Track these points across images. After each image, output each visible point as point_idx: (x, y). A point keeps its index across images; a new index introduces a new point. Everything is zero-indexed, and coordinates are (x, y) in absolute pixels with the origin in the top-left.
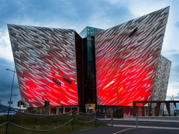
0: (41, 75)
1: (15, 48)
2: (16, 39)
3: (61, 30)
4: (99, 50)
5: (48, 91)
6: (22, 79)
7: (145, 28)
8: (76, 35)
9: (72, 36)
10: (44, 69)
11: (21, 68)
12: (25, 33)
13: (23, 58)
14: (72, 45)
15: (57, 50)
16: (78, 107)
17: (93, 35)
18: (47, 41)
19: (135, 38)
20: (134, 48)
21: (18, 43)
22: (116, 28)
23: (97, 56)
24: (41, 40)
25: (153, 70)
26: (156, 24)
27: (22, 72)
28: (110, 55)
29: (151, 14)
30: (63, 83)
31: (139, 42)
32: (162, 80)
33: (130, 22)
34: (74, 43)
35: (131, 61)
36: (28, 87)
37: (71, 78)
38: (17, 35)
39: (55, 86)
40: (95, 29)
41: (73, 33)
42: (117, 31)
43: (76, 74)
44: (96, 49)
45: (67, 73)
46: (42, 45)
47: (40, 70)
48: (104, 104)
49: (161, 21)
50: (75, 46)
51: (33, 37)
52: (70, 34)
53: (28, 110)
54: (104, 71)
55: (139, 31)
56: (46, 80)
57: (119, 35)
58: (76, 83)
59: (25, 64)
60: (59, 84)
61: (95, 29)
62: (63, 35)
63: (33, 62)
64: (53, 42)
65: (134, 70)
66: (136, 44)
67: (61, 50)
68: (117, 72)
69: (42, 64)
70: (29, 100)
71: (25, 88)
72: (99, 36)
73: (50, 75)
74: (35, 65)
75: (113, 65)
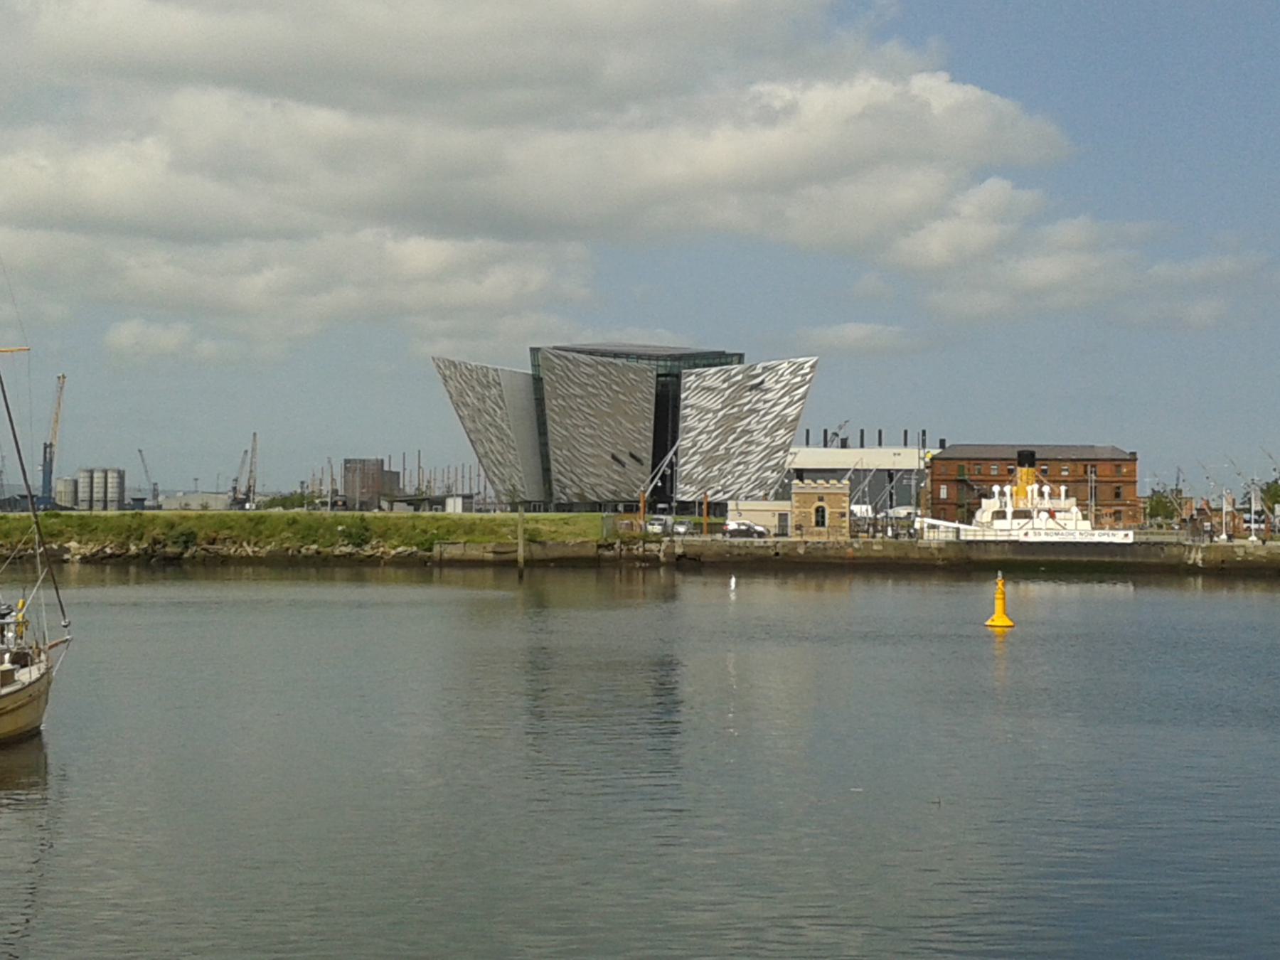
23: (683, 412)
47: (591, 436)
55: (766, 385)
66: (760, 405)
70: (568, 491)
72: (693, 378)
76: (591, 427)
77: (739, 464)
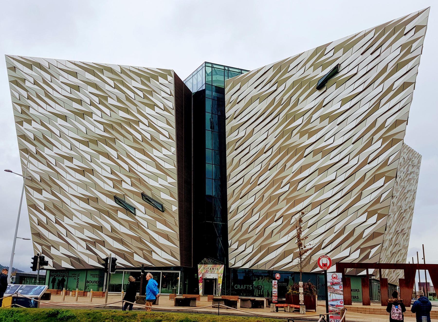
0: (85, 186)
1: (24, 116)
2: (25, 94)
3: (139, 70)
4: (234, 123)
5: (101, 228)
6: (36, 195)
7: (361, 66)
8: (179, 85)
9: (169, 88)
10: (92, 171)
11: (37, 168)
12: (48, 77)
13: (42, 141)
14: (165, 109)
15: (129, 122)
16: (180, 272)
17: (221, 85)
18: (103, 99)
19: (332, 91)
20: (331, 117)
21: (29, 101)
22: (282, 67)
24: (87, 94)
25: (384, 179)
26: (391, 54)
27: (38, 178)
28: (265, 136)
29: (377, 29)
30: (142, 208)
31: (344, 101)
32: (399, 204)
33: (320, 51)
34: (171, 104)
35: (325, 152)
36: (52, 217)
37: (164, 196)
38: (27, 84)
39: (121, 215)
40: (227, 69)
41: (171, 79)
42: (286, 72)
43: (176, 185)
44: (227, 121)
45: (151, 182)
46: (92, 107)
47: (83, 172)
48: (247, 266)
49: (407, 48)
50: (173, 112)
51: (68, 89)
52: (161, 80)
53: (50, 275)
54: (247, 178)
56: (97, 200)
57: (289, 83)
58: (175, 208)
59: (46, 159)
60: (130, 210)
61: (227, 71)
62: (143, 83)
63: (65, 151)
64: (119, 100)
65: (332, 177)
66: (335, 106)
67: (138, 122)
68: (285, 181)
69: (88, 157)
70: (53, 251)
71: (44, 219)
73: (109, 187)
74: (70, 159)
75: (272, 163)
76: (83, 159)
77: (314, 205)
